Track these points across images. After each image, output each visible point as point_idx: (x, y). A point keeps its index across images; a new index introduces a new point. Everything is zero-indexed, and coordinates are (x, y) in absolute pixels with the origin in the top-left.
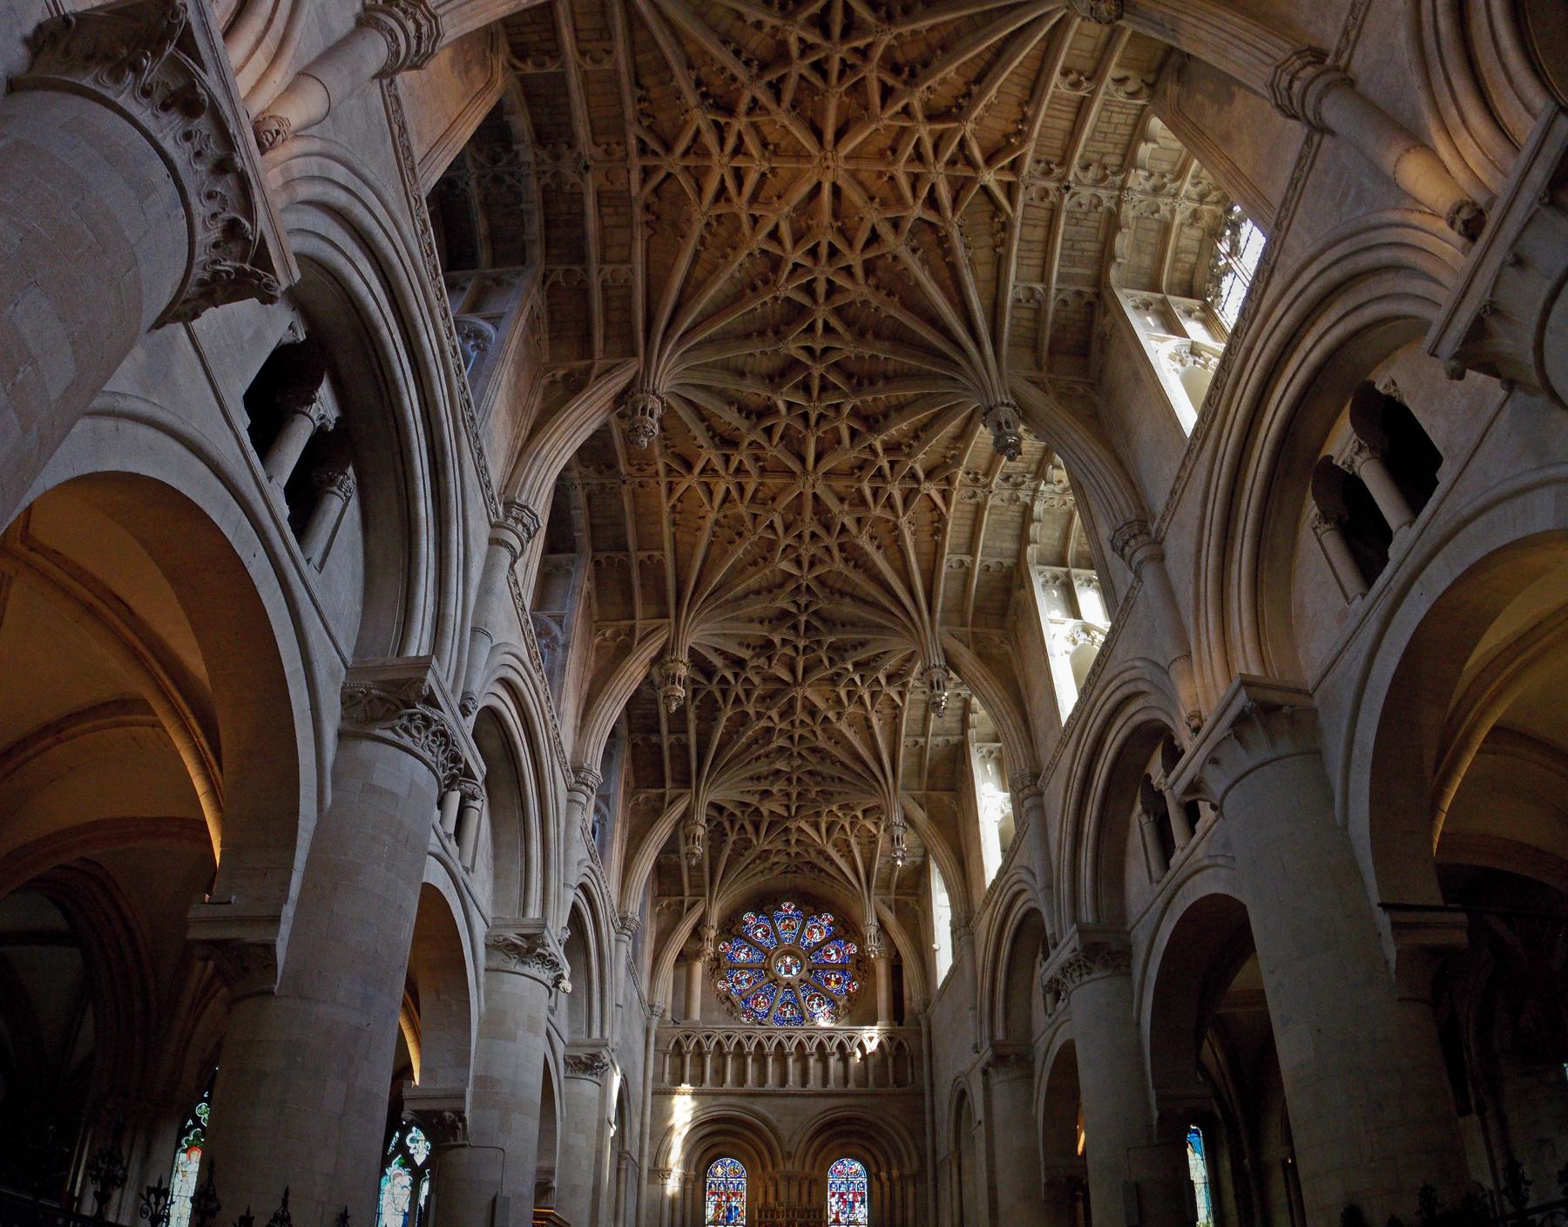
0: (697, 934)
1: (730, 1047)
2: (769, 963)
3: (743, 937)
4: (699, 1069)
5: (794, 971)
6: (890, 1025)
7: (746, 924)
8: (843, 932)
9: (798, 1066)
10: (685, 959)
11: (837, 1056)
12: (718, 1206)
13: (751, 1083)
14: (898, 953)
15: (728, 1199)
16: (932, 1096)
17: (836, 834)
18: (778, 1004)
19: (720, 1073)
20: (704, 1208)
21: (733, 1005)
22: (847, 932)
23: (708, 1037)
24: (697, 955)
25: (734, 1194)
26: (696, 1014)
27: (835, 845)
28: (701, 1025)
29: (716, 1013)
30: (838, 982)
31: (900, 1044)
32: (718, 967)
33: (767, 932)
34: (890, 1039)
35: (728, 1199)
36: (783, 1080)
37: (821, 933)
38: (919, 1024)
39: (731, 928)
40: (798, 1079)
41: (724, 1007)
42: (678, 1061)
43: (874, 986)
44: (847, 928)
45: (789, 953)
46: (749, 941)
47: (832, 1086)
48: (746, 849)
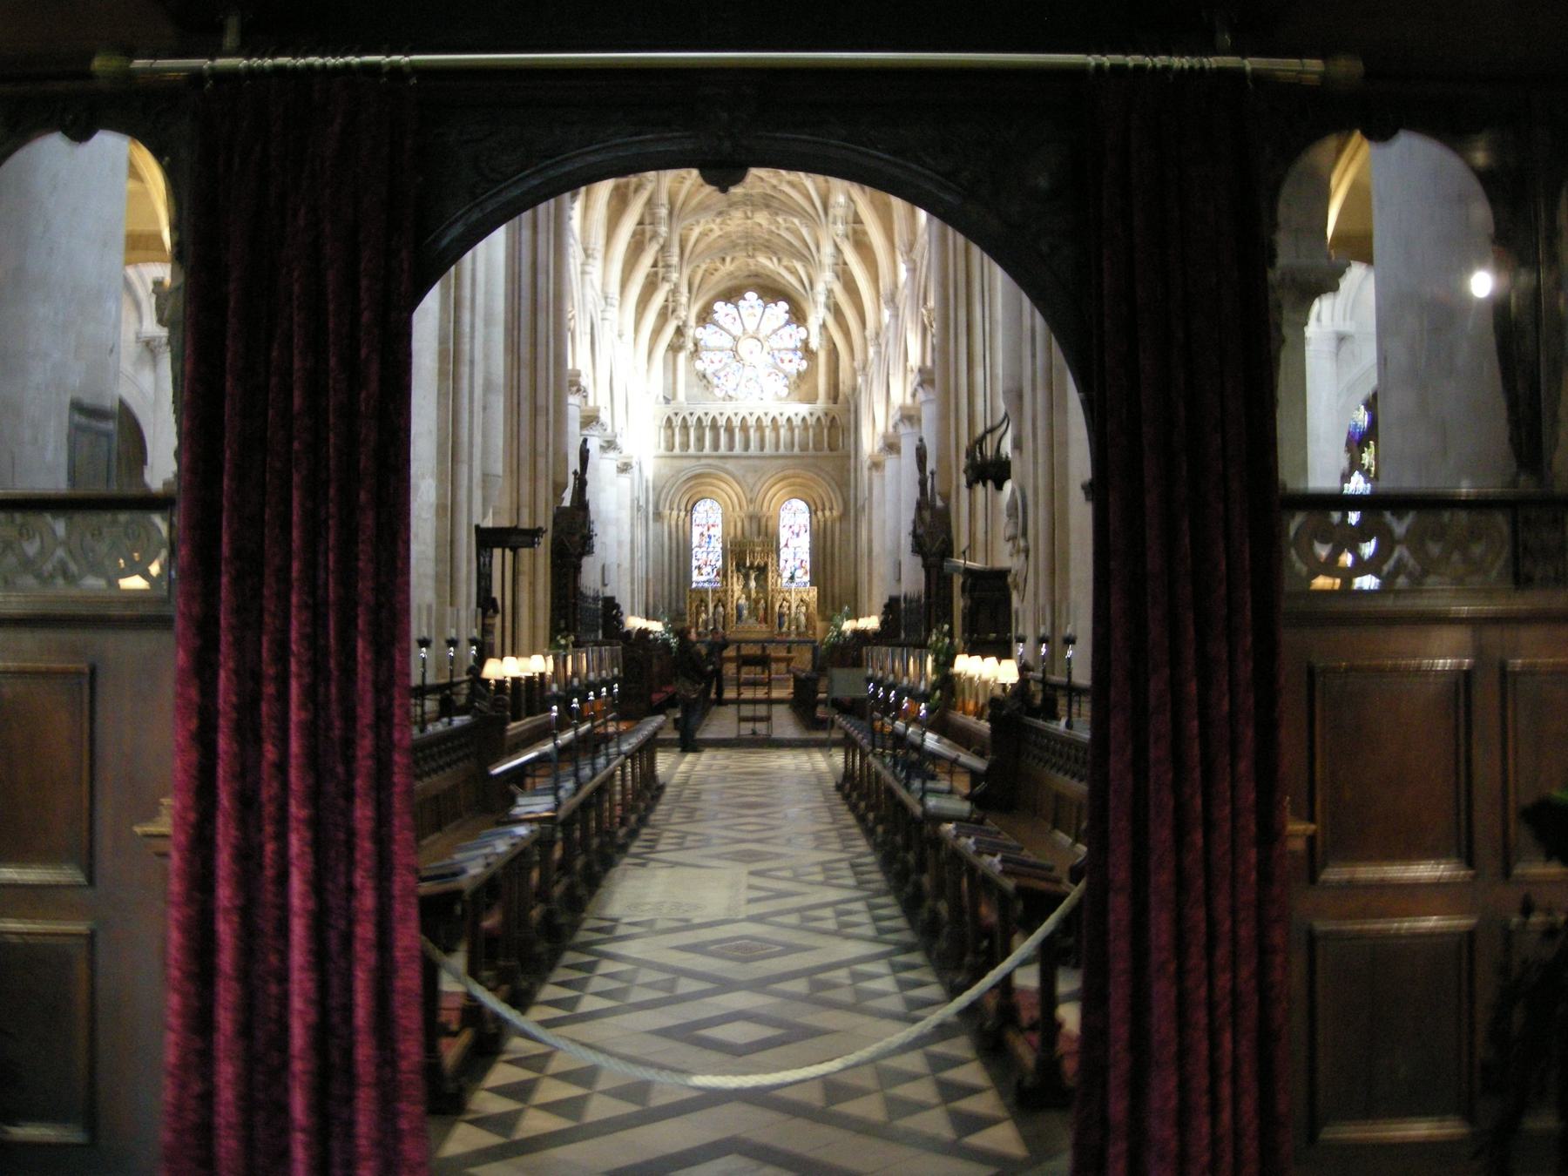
0: (680, 331)
1: (707, 422)
3: (715, 323)
6: (827, 403)
9: (758, 434)
10: (674, 348)
11: (787, 427)
12: (702, 534)
13: (723, 449)
14: (834, 344)
16: (856, 458)
17: (785, 262)
18: (743, 381)
21: (708, 382)
22: (798, 319)
26: (681, 395)
29: (696, 389)
31: (834, 418)
32: (696, 351)
34: (826, 414)
36: (747, 446)
38: (848, 402)
39: (705, 317)
43: (817, 366)
44: (798, 316)
45: (752, 337)
46: (721, 328)
47: (782, 450)
48: (716, 270)
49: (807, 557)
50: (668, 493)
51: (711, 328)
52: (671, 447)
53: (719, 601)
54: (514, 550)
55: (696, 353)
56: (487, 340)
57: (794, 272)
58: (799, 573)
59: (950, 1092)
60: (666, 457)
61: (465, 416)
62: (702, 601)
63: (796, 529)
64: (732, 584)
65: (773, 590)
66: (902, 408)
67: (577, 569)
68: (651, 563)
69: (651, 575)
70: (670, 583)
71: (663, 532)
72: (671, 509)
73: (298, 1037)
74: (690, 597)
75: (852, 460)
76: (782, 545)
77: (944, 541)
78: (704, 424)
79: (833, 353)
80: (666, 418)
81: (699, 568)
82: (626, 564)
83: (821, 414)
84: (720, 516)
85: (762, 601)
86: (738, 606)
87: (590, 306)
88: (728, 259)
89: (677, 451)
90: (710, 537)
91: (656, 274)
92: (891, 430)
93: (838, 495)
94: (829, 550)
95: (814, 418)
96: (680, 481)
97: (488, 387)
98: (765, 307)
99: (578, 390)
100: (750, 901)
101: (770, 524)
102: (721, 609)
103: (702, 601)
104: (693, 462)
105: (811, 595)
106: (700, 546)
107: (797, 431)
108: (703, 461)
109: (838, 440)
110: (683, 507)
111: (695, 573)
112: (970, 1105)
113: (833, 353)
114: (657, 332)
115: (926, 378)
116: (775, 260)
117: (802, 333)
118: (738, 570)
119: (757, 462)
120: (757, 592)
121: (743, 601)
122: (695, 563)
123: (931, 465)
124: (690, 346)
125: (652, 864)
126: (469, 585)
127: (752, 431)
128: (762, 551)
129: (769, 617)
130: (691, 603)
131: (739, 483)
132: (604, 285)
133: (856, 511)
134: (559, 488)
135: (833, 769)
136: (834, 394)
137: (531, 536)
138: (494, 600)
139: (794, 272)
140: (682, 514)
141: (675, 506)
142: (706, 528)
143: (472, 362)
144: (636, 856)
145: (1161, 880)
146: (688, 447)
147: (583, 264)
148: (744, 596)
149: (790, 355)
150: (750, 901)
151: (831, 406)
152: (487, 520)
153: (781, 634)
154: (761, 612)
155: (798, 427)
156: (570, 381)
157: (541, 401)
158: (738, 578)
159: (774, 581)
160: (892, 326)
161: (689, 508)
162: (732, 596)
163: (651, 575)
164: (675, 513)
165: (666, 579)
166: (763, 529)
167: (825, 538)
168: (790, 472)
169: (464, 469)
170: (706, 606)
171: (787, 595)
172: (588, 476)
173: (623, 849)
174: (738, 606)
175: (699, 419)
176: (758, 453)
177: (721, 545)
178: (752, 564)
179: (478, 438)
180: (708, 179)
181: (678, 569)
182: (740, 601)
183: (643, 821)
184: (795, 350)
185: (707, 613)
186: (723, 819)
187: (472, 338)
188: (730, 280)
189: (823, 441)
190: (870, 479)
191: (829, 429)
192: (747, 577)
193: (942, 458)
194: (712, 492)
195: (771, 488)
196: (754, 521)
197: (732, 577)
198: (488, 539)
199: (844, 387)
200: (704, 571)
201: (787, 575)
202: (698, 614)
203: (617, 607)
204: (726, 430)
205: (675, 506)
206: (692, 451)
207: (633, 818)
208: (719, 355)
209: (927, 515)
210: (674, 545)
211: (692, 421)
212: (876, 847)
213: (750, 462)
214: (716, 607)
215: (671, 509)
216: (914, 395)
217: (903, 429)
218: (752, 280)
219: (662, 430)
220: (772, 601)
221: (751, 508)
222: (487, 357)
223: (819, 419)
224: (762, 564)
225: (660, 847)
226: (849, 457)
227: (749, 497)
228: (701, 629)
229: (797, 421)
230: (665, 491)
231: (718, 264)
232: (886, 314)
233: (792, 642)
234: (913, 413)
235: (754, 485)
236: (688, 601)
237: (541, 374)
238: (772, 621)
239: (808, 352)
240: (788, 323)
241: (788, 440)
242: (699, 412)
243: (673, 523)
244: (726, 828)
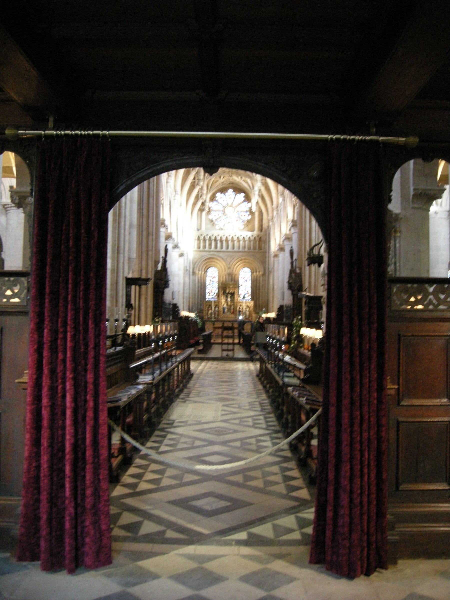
0: (203, 204)
1: (213, 238)
3: (217, 201)
9: (232, 243)
10: (201, 210)
17: (243, 178)
19: (210, 245)
27: (243, 180)
31: (260, 238)
36: (228, 248)
42: (199, 242)
44: (248, 199)
45: (231, 206)
51: (215, 203)
52: (199, 247)
54: (140, 286)
55: (209, 212)
56: (131, 208)
57: (246, 182)
58: (246, 296)
59: (287, 479)
61: (122, 236)
66: (286, 235)
67: (163, 293)
72: (199, 271)
73: (68, 448)
75: (267, 254)
77: (299, 286)
78: (212, 239)
79: (261, 213)
82: (181, 291)
83: (255, 236)
87: (169, 195)
88: (222, 177)
91: (194, 182)
92: (281, 243)
95: (253, 237)
96: (202, 261)
97: (131, 226)
98: (236, 195)
99: (164, 226)
100: (222, 415)
101: (236, 277)
104: (207, 253)
108: (211, 253)
110: (203, 270)
112: (294, 483)
113: (261, 213)
114: (195, 204)
115: (294, 224)
116: (240, 177)
117: (249, 205)
119: (231, 254)
120: (231, 303)
121: (225, 306)
122: (207, 291)
123: (295, 257)
124: (207, 209)
125: (187, 402)
126: (123, 299)
132: (175, 186)
134: (156, 263)
135: (256, 369)
136: (261, 228)
137: (146, 281)
138: (132, 305)
139: (246, 182)
140: (203, 273)
143: (125, 216)
144: (182, 399)
145: (346, 402)
147: (167, 179)
149: (245, 213)
150: (222, 415)
151: (260, 233)
152: (129, 275)
154: (232, 310)
156: (161, 223)
157: (150, 230)
160: (283, 203)
166: (233, 279)
167: (257, 282)
169: (121, 256)
170: (211, 307)
172: (168, 258)
173: (177, 396)
175: (210, 237)
177: (218, 284)
179: (127, 245)
180: (206, 171)
183: (185, 386)
184: (247, 211)
186: (215, 386)
187: (125, 207)
188: (223, 185)
190: (274, 261)
192: (227, 297)
193: (299, 254)
198: (130, 282)
199: (265, 226)
201: (242, 296)
202: (208, 310)
203: (177, 307)
206: (207, 249)
207: (181, 385)
208: (218, 213)
209: (293, 275)
211: (207, 238)
212: (269, 397)
213: (229, 253)
214: (215, 308)
215: (199, 271)
216: (290, 230)
217: (286, 243)
218: (231, 185)
222: (131, 215)
223: (255, 238)
225: (190, 396)
229: (247, 239)
230: (197, 264)
231: (218, 179)
232: (281, 199)
234: (289, 237)
237: (151, 221)
239: (251, 213)
240: (244, 201)
241: (243, 245)
242: (210, 235)
244: (216, 389)
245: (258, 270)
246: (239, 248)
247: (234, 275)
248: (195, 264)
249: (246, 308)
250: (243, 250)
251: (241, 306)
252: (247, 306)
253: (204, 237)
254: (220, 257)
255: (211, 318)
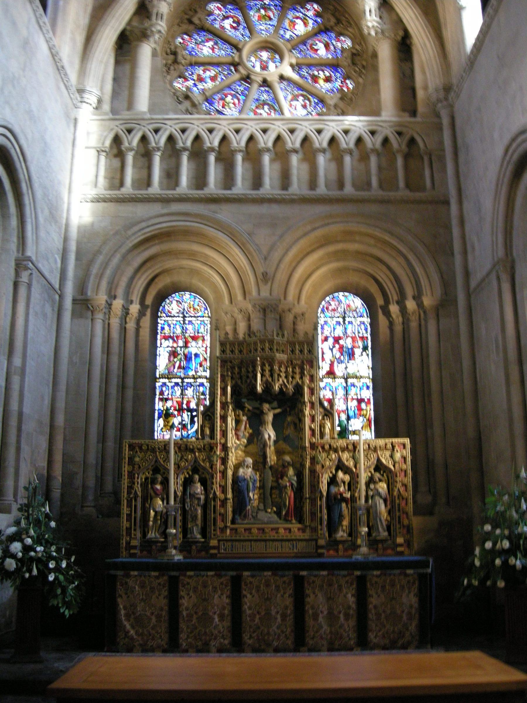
2: (240, 57)
4: (145, 172)
5: (271, 66)
6: (399, 116)
7: (210, 14)
8: (333, 21)
9: (277, 166)
12: (173, 354)
15: (186, 343)
20: (154, 356)
23: (156, 131)
24: (144, 35)
25: (194, 338)
28: (148, 116)
30: (328, 80)
31: (412, 141)
32: (175, 62)
33: (238, 23)
35: (186, 343)
37: (306, 24)
40: (277, 183)
41: (182, 107)
42: (117, 162)
49: (367, 394)
50: (105, 265)
53: (196, 470)
58: (356, 424)
60: (105, 200)
62: (156, 470)
63: (348, 343)
64: (224, 434)
65: (313, 446)
68: (62, 395)
69: (60, 419)
70: (103, 438)
71: (92, 336)
74: (131, 460)
76: (322, 372)
78: (180, 144)
80: (111, 136)
81: (167, 415)
83: (388, 132)
84: (207, 320)
85: (291, 472)
86: (236, 479)
89: (128, 188)
90: (188, 358)
93: (432, 269)
94: (416, 374)
95: (379, 139)
101: (302, 328)
102: (198, 488)
103: (156, 470)
104: (157, 208)
105: (398, 456)
106: (169, 376)
107: (347, 159)
108: (175, 207)
109: (422, 176)
110: (136, 297)
111: (160, 423)
118: (238, 406)
119: (275, 209)
120: (279, 453)
121: (247, 472)
122: (159, 406)
127: (266, 159)
128: (290, 362)
129: (307, 507)
130: (131, 475)
131: (241, 247)
133: (468, 295)
140: (135, 308)
141: (120, 292)
142: (181, 343)
146: (149, 184)
148: (249, 461)
151: (407, 118)
153: (334, 544)
155: (350, 152)
158: (238, 422)
159: (316, 426)
161: (149, 301)
162: (224, 461)
163: (60, 419)
164: (118, 304)
165: (94, 430)
168: (335, 228)
170: (165, 482)
171: (345, 456)
174: (236, 479)
175: (171, 139)
176: (278, 192)
177: (207, 374)
178: (268, 387)
181: (122, 413)
182: (241, 471)
184: (334, 66)
185: (166, 498)
189: (396, 178)
191: (407, 157)
194: (194, 272)
195: (299, 263)
196: (270, 316)
197: (224, 418)
200: (176, 421)
202: (147, 499)
204: (217, 159)
205: (120, 292)
210: (115, 360)
213: (264, 209)
214: (188, 483)
219: (103, 159)
220: (313, 472)
221: (265, 293)
223: (386, 141)
224: (291, 388)
226: (447, 203)
227: (260, 270)
228: (152, 535)
230: (100, 259)
233: (365, 566)
235: (272, 248)
236: (126, 468)
238: (313, 514)
241: (333, 176)
243: (115, 322)
245: (409, 291)
246: (313, 184)
247: (289, 318)
248: (91, 262)
249: (371, 481)
250: (335, 193)
251: (340, 466)
252: (379, 467)
253: (144, 139)
254: (221, 227)
255: (164, 548)
